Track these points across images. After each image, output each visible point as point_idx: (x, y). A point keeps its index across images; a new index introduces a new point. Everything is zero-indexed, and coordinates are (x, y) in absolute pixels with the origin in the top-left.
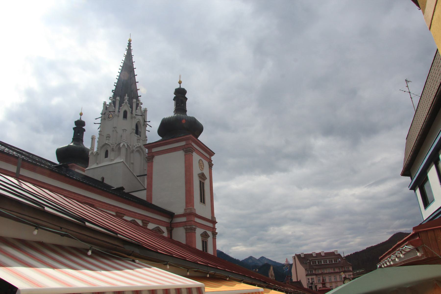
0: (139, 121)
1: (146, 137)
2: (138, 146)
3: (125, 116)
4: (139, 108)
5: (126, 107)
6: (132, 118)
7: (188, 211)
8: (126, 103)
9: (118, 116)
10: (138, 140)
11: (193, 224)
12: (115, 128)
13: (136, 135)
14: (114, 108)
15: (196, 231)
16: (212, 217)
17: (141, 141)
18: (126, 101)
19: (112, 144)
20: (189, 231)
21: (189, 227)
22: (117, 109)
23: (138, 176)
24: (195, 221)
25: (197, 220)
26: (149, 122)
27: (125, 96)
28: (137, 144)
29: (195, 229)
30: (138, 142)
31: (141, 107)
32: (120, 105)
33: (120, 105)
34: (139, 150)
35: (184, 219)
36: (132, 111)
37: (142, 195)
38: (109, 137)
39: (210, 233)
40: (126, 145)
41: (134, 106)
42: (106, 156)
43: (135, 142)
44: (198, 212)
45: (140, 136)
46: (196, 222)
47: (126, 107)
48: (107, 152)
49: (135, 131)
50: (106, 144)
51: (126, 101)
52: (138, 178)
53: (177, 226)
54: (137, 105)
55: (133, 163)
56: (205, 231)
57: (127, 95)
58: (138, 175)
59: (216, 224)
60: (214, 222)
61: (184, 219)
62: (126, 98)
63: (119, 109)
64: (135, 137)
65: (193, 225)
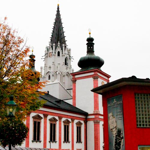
0: (66, 57)
1: (71, 66)
3: (59, 55)
4: (66, 49)
5: (59, 49)
6: (62, 56)
8: (59, 47)
9: (55, 55)
10: (66, 68)
12: (53, 62)
13: (65, 66)
14: (52, 50)
17: (68, 69)
18: (59, 45)
19: (52, 72)
20: (96, 123)
21: (96, 121)
22: (54, 51)
23: (67, 90)
27: (58, 43)
28: (66, 71)
30: (66, 70)
31: (67, 48)
32: (56, 49)
33: (56, 49)
34: (68, 75)
35: (93, 117)
36: (62, 51)
37: (70, 102)
38: (50, 68)
40: (60, 73)
41: (64, 48)
42: (49, 79)
43: (64, 70)
45: (68, 66)
47: (59, 49)
48: (49, 76)
49: (65, 64)
50: (49, 72)
51: (59, 45)
52: (67, 91)
53: (89, 120)
54: (65, 47)
55: (64, 83)
58: (67, 89)
61: (93, 117)
63: (55, 51)
64: (65, 67)
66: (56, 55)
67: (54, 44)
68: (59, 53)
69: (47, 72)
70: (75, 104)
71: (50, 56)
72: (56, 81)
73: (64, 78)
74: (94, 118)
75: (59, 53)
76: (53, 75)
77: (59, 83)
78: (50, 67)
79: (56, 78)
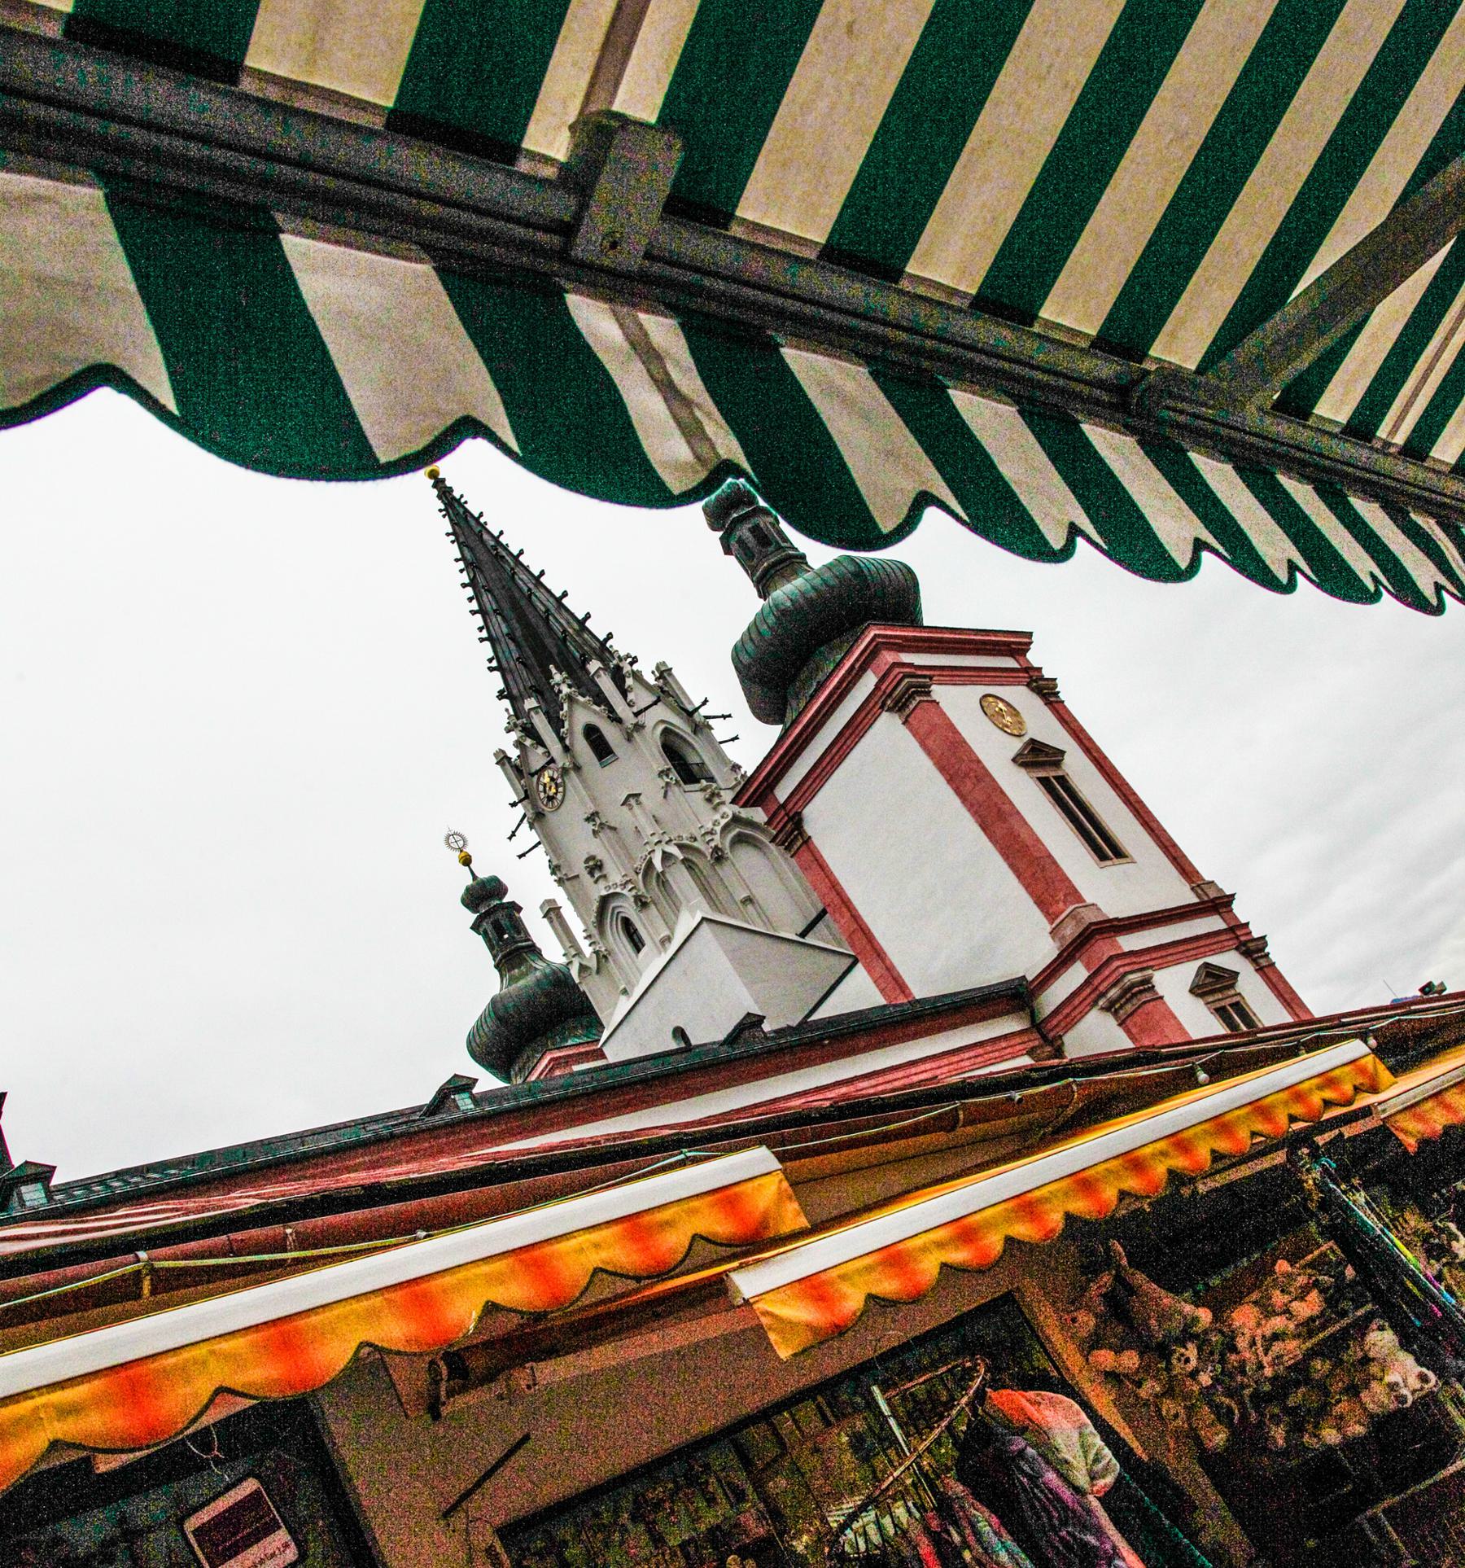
0: (666, 732)
2: (723, 822)
3: (602, 749)
4: (629, 682)
5: (583, 715)
6: (629, 738)
7: (1070, 931)
8: (570, 698)
9: (577, 768)
10: (709, 800)
11: (1122, 970)
14: (540, 750)
15: (1160, 990)
16: (1192, 889)
18: (565, 690)
19: (624, 885)
21: (1114, 993)
22: (556, 749)
23: (803, 934)
24: (1126, 950)
25: (1130, 942)
26: (705, 702)
28: (717, 817)
29: (1147, 985)
30: (715, 809)
31: (637, 676)
33: (556, 723)
35: (1076, 975)
36: (611, 710)
38: (599, 866)
39: (1229, 960)
44: (1116, 908)
45: (711, 779)
46: (1132, 953)
47: (583, 715)
48: (627, 924)
49: (674, 775)
51: (565, 690)
52: (809, 940)
55: (748, 900)
56: (1200, 962)
57: (554, 671)
59: (1233, 906)
60: (1220, 904)
61: (1076, 975)
62: (558, 684)
63: (562, 739)
64: (693, 798)
65: (1126, 973)
66: (581, 761)
67: (530, 703)
68: (592, 733)
69: (595, 905)
70: (902, 987)
71: (551, 799)
72: (686, 923)
73: (725, 871)
74: (1087, 982)
75: (592, 734)
76: (642, 903)
77: (705, 924)
78: (595, 867)
79: (676, 908)
